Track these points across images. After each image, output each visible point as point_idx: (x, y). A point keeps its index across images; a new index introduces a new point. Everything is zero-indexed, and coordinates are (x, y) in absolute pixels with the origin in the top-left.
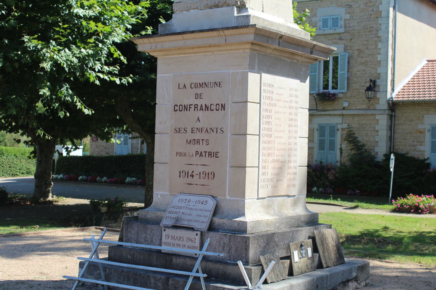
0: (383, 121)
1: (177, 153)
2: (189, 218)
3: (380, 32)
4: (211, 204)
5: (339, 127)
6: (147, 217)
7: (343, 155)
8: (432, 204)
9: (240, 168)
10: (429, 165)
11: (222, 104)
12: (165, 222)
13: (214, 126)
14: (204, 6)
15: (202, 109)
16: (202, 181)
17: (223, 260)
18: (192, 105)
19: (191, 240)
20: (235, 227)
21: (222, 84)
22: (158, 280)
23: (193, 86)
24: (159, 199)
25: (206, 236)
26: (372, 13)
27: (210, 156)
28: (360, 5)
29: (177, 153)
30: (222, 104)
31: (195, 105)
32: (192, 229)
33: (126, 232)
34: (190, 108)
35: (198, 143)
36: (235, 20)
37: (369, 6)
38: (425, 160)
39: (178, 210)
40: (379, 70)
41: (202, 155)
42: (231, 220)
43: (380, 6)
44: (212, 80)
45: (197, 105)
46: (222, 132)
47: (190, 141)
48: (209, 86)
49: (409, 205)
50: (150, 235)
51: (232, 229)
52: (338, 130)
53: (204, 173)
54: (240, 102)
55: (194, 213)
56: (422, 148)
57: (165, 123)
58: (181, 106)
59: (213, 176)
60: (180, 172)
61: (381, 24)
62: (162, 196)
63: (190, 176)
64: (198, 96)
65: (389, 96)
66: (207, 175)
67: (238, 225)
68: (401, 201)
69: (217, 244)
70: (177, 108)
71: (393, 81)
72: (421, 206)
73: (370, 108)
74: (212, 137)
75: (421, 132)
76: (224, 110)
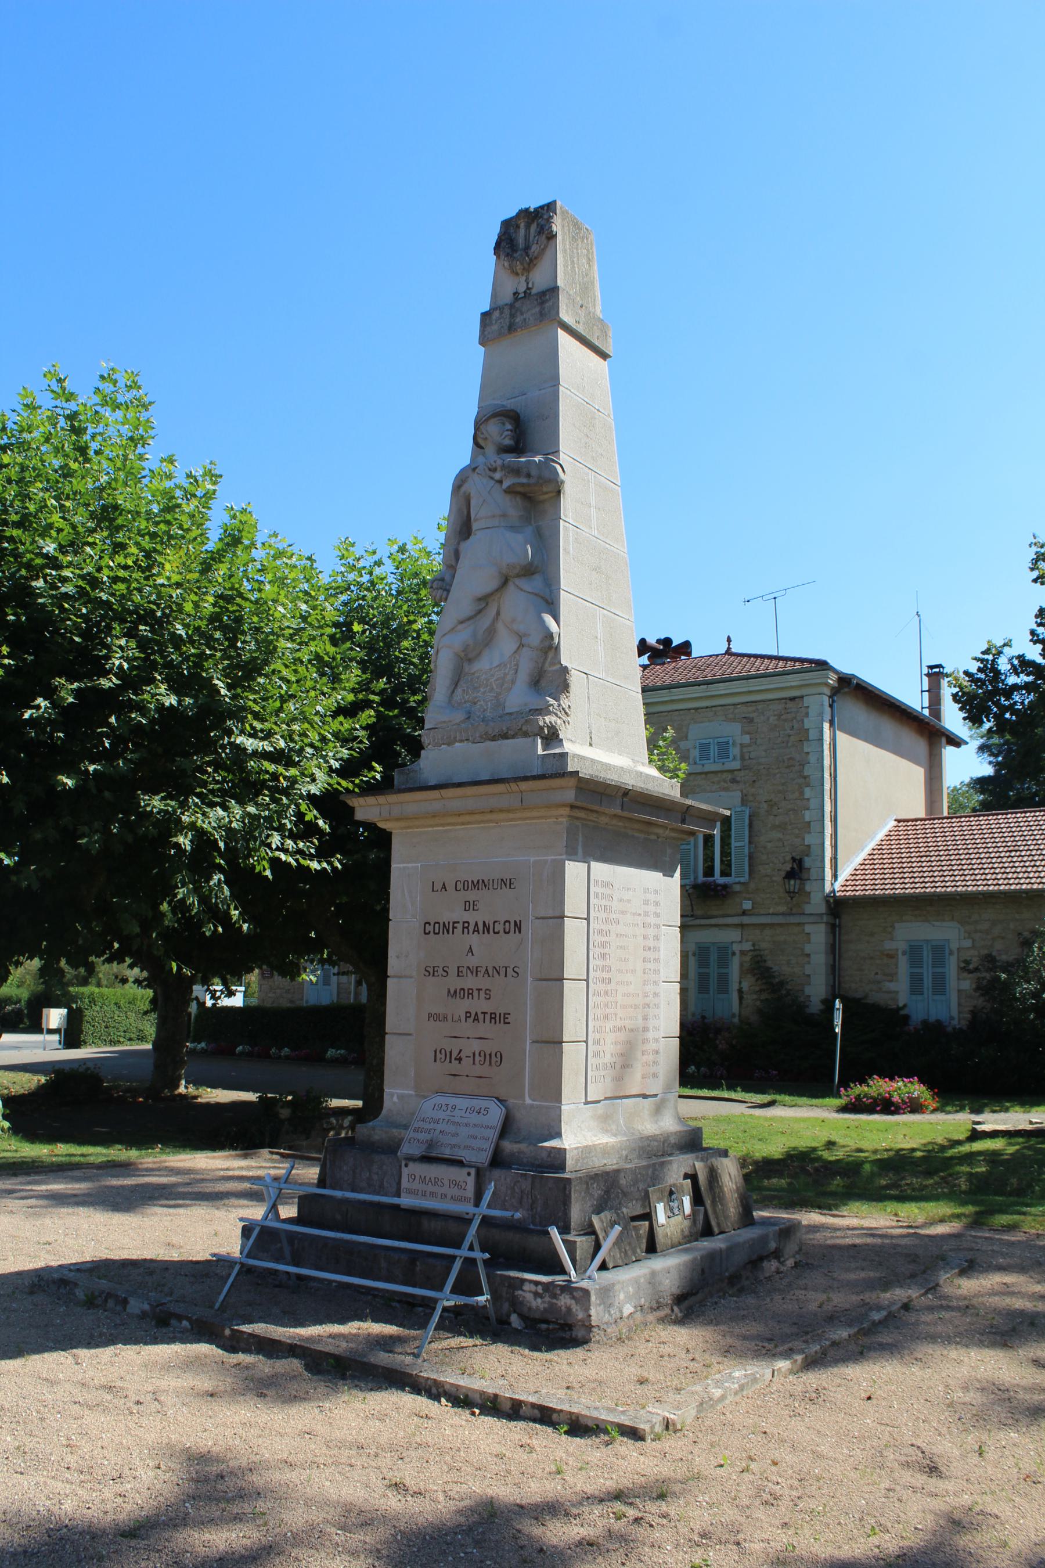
0: (818, 935)
1: (430, 1015)
2: (454, 1141)
3: (806, 768)
4: (496, 1115)
5: (736, 948)
7: (744, 1002)
8: (916, 1094)
10: (907, 1018)
12: (406, 1149)
15: (478, 931)
16: (478, 1070)
20: (542, 1159)
23: (460, 886)
24: (394, 1103)
26: (791, 732)
28: (768, 719)
29: (430, 1015)
32: (459, 1163)
34: (454, 928)
37: (785, 720)
38: (899, 1009)
39: (432, 1126)
40: (809, 839)
42: (535, 1145)
43: (806, 720)
47: (455, 992)
49: (872, 1098)
51: (537, 1162)
52: (734, 954)
53: (482, 1054)
56: (892, 986)
58: (437, 925)
61: (808, 753)
62: (401, 1097)
64: (469, 906)
65: (828, 889)
67: (549, 1156)
68: (858, 1089)
70: (429, 928)
71: (834, 859)
72: (896, 1098)
73: (794, 911)
75: (890, 956)
76: (520, 932)
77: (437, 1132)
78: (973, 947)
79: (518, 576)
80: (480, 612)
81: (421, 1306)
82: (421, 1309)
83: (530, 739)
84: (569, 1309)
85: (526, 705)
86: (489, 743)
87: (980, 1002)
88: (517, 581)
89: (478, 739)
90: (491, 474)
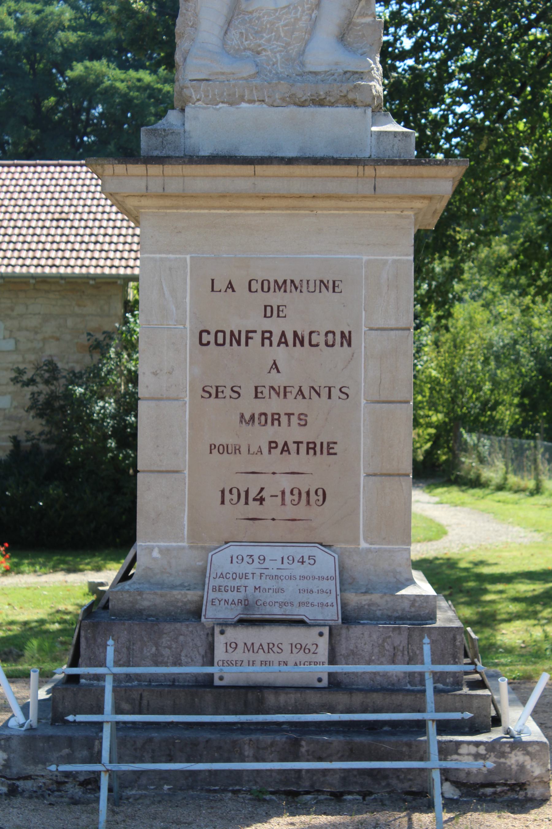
1: (212, 447)
2: (280, 597)
4: (326, 563)
6: (137, 606)
9: (397, 478)
11: (342, 333)
12: (210, 613)
13: (320, 382)
15: (286, 343)
16: (290, 511)
17: (393, 685)
18: (255, 332)
19: (303, 648)
20: (403, 610)
21: (341, 287)
22: (265, 748)
23: (254, 286)
24: (155, 559)
25: (344, 636)
27: (312, 452)
29: (212, 447)
30: (342, 333)
31: (263, 332)
32: (301, 623)
33: (88, 646)
34: (247, 338)
35: (276, 423)
36: (374, 142)
39: (238, 582)
41: (288, 451)
42: (393, 595)
44: (314, 275)
45: (271, 332)
46: (344, 396)
47: (252, 417)
48: (304, 289)
50: (170, 647)
51: (396, 614)
53: (296, 492)
54: (392, 329)
55: (290, 586)
57: (170, 373)
58: (220, 335)
59: (321, 498)
60: (223, 492)
63: (255, 500)
64: (268, 311)
66: (304, 496)
67: (413, 605)
69: (376, 650)
74: (316, 407)
76: (349, 345)
77: (250, 590)
78: (16, 350)
81: (307, 793)
82: (309, 797)
83: (359, 111)
84: (522, 767)
85: (336, 64)
87: (37, 426)
89: (278, 102)
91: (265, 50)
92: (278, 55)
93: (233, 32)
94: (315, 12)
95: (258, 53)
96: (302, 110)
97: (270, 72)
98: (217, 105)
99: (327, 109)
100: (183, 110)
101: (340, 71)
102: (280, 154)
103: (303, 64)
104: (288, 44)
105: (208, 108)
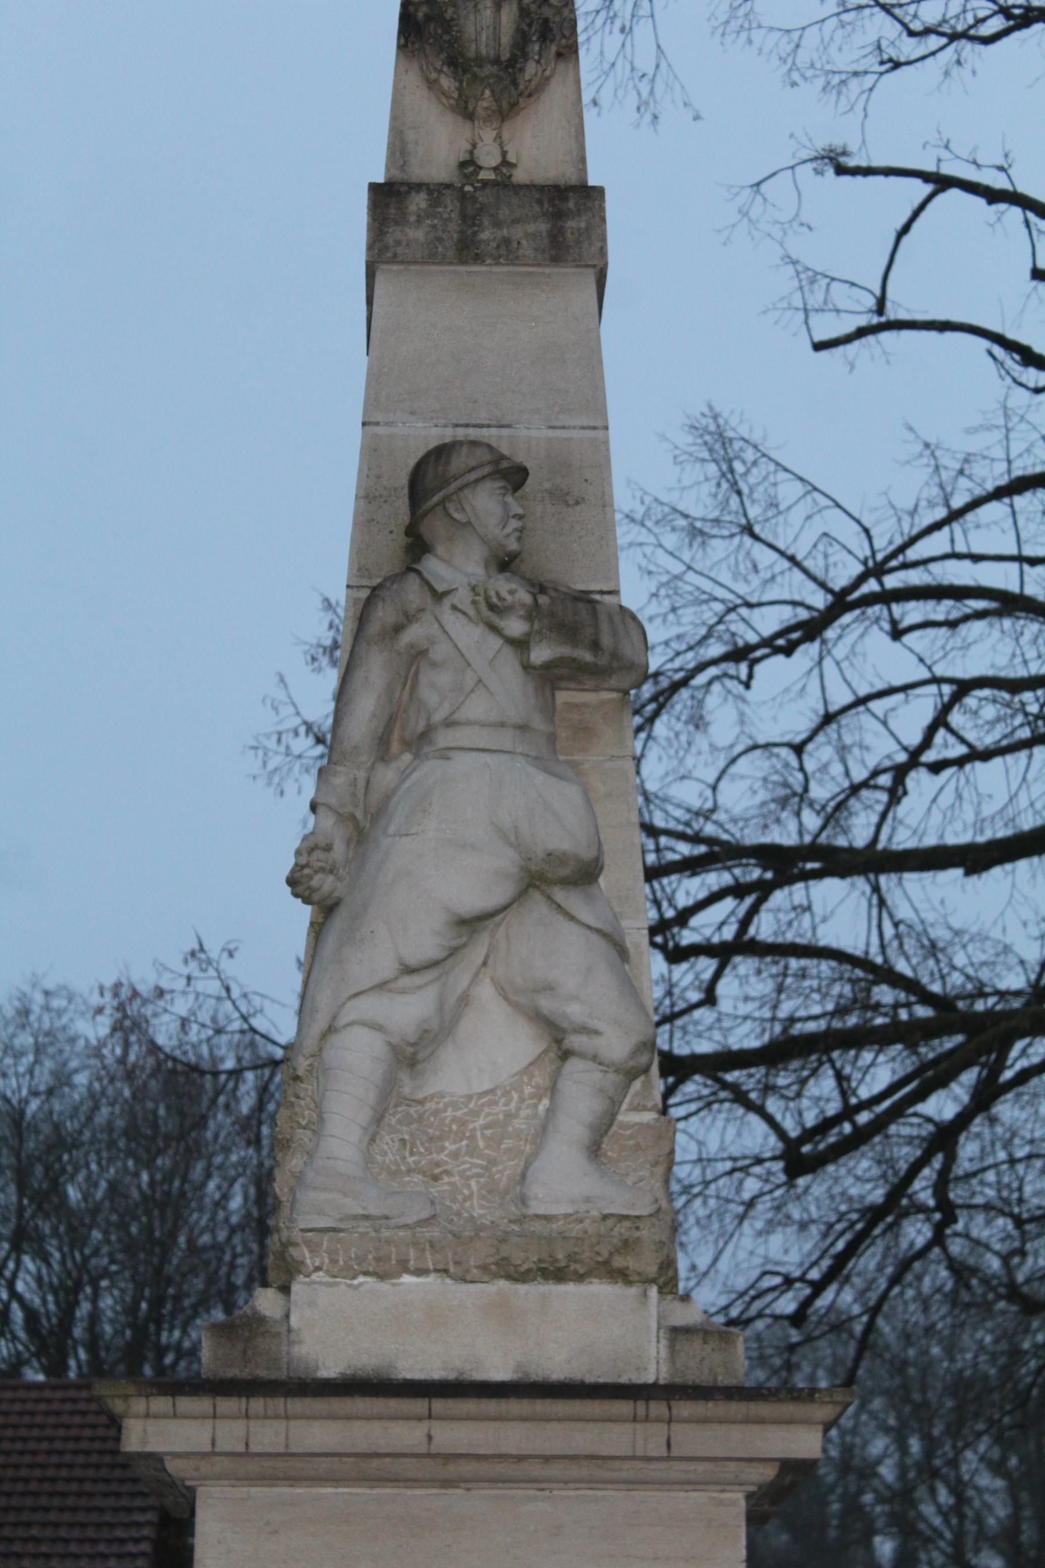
14: (484, 1268)
79: (567, 882)
80: (453, 952)
83: (634, 1291)
85: (587, 1200)
86: (502, 1284)
88: (560, 895)
90: (495, 619)
91: (447, 1173)
92: (473, 1183)
93: (387, 1139)
94: (546, 1102)
95: (436, 1178)
96: (522, 1289)
97: (459, 1214)
98: (354, 1278)
99: (570, 1287)
100: (285, 1289)
101: (595, 1213)
102: (479, 1376)
103: (523, 1200)
104: (492, 1162)
105: (337, 1284)
